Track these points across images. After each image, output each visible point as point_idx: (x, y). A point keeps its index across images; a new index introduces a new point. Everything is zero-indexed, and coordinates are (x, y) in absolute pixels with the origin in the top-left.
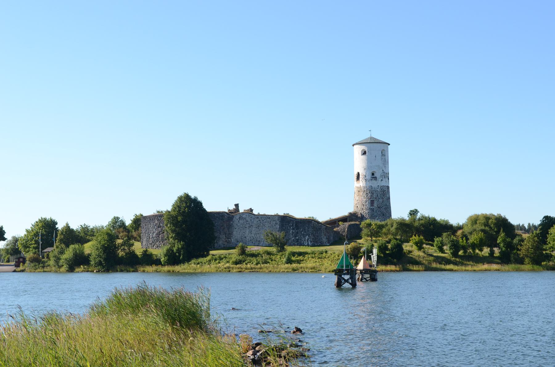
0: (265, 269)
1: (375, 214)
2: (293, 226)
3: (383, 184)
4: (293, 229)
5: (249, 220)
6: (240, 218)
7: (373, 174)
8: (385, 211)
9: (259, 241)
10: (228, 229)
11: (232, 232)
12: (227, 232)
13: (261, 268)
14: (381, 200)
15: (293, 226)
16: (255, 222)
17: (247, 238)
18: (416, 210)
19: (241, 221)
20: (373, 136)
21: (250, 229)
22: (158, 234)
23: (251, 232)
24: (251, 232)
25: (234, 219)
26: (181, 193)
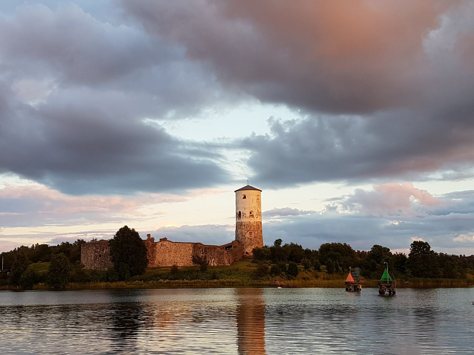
0: (198, 284)
3: (258, 220)
4: (203, 253)
5: (169, 247)
7: (251, 213)
10: (152, 253)
11: (155, 257)
12: (152, 256)
13: (194, 283)
14: (256, 232)
15: (202, 251)
16: (173, 248)
18: (280, 240)
21: (170, 253)
22: (96, 257)
25: (157, 245)
26: (122, 226)
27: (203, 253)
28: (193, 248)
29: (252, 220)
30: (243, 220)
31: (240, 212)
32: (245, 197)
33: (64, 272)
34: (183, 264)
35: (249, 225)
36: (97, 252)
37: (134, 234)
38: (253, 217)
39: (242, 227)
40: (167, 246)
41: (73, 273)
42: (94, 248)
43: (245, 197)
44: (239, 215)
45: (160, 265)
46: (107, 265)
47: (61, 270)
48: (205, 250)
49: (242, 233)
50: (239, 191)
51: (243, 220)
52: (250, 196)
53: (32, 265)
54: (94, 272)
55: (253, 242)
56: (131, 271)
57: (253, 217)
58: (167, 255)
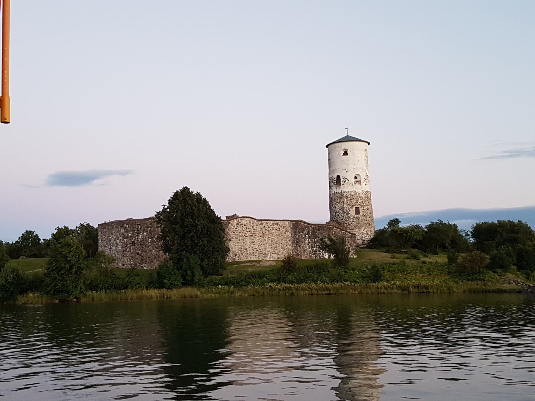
1: (361, 223)
2: (308, 233)
4: (309, 238)
5: (250, 227)
6: (237, 224)
7: (356, 178)
8: (370, 220)
9: (265, 254)
14: (366, 208)
15: (308, 233)
16: (259, 229)
17: (248, 249)
18: (397, 219)
19: (239, 229)
20: (349, 135)
21: (252, 238)
22: (125, 247)
23: (253, 242)
24: (253, 242)
27: (309, 238)
28: (292, 228)
29: (359, 189)
30: (345, 189)
31: (338, 177)
32: (346, 153)
33: (76, 272)
34: (275, 256)
35: (353, 197)
36: (128, 237)
37: (200, 203)
38: (360, 184)
39: (342, 200)
40: (248, 225)
41: (92, 273)
42: (122, 231)
43: (346, 153)
44: (336, 181)
45: (236, 258)
46: (155, 259)
47: (71, 267)
48: (313, 232)
49: (343, 209)
50: (337, 144)
51: (345, 189)
52: (355, 151)
53: (13, 263)
54: (132, 272)
55: (361, 223)
56: (202, 268)
57: (360, 184)
58: (248, 241)
